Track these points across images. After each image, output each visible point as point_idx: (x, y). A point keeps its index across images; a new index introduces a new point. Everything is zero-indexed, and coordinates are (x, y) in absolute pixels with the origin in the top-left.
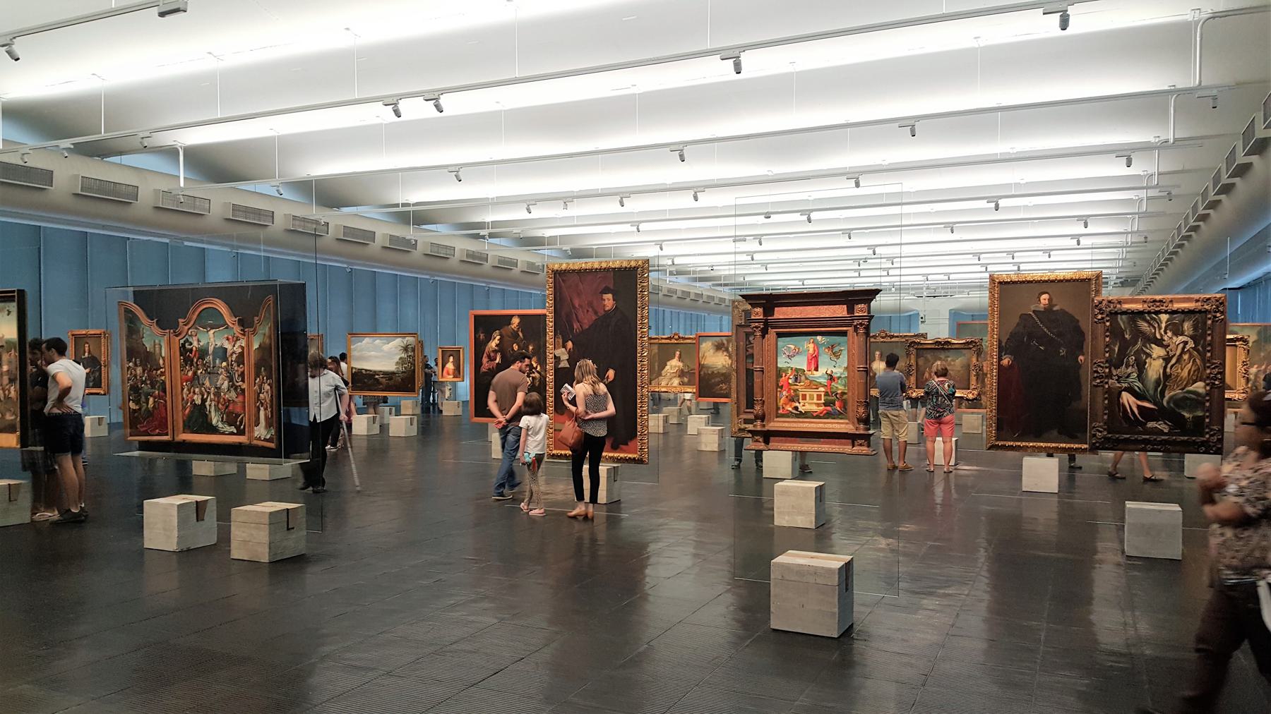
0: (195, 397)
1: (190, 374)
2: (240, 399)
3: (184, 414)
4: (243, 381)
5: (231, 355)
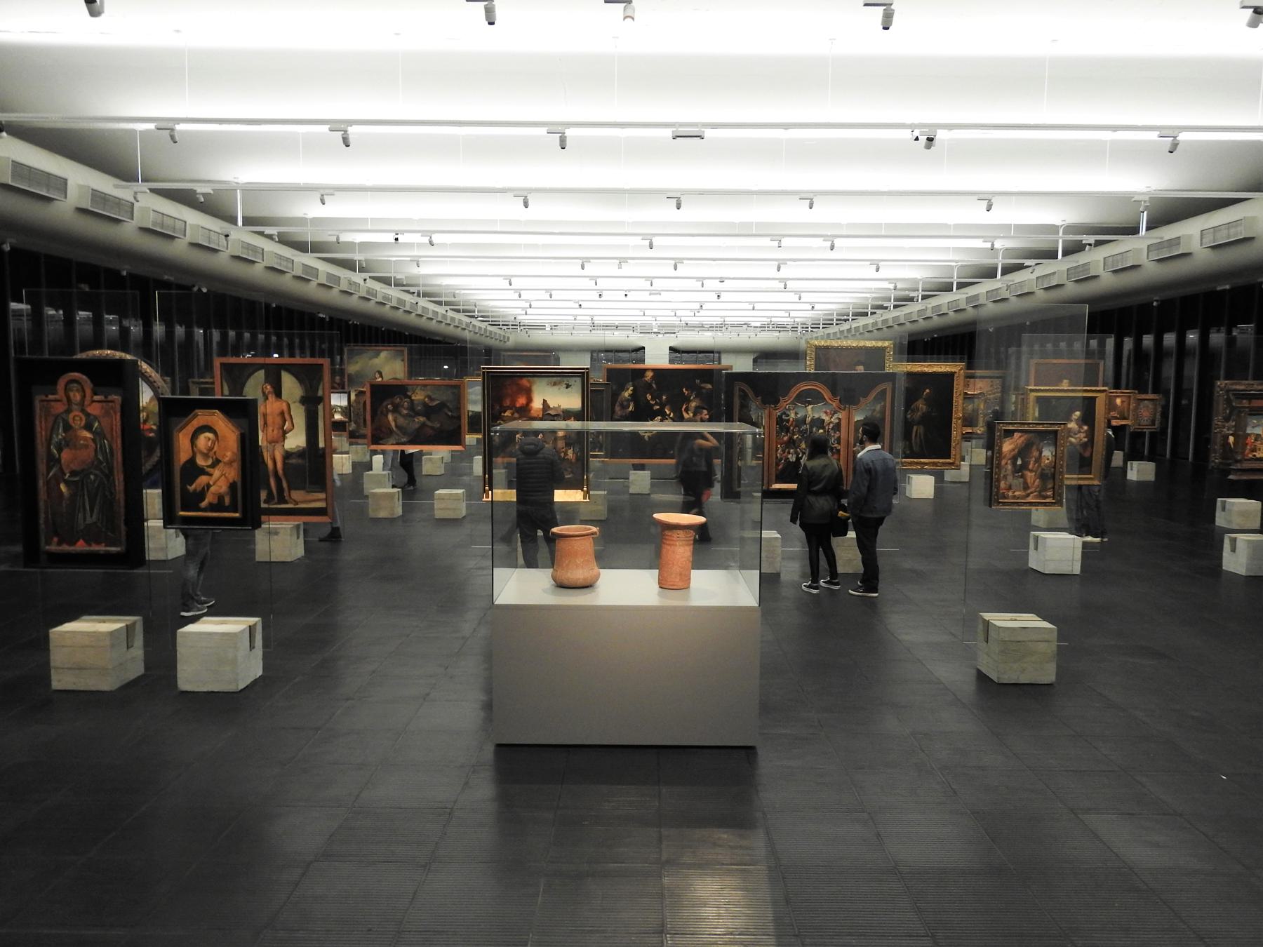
0: (790, 456)
1: (786, 438)
2: (836, 456)
3: (777, 470)
4: (839, 443)
5: (829, 424)
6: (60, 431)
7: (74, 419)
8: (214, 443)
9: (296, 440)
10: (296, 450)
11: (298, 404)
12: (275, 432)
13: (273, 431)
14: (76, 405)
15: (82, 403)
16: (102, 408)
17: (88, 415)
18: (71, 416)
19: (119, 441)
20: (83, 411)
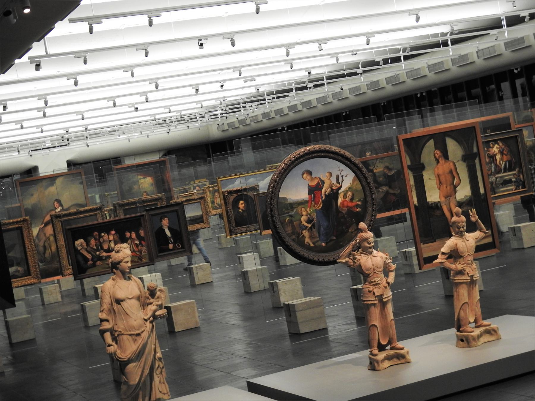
10: (465, 199)
11: (461, 162)
12: (448, 188)
13: (447, 187)
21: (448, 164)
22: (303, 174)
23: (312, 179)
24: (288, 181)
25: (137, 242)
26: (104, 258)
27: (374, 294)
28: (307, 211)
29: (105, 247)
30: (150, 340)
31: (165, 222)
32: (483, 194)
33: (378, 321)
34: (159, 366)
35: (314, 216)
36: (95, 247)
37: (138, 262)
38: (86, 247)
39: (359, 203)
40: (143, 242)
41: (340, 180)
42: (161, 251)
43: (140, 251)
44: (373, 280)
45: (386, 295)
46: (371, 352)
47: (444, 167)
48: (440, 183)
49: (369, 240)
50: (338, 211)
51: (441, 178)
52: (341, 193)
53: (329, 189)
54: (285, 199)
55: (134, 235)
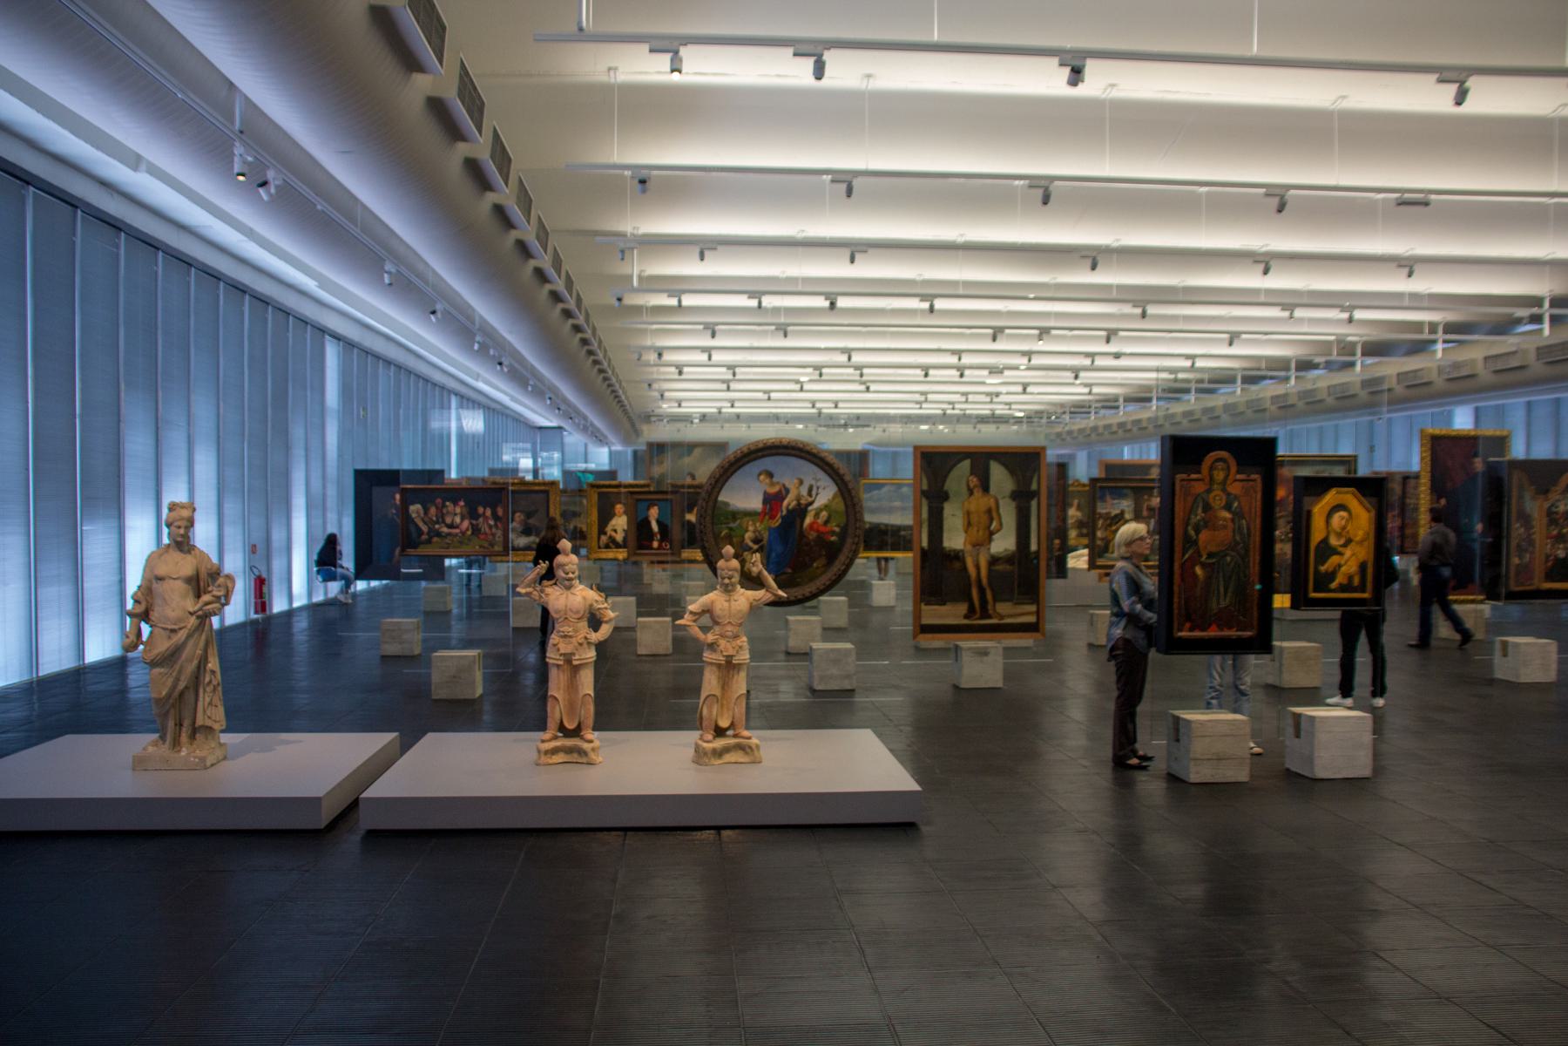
6: (1200, 510)
7: (1215, 499)
8: (1347, 521)
9: (1004, 543)
11: (1008, 501)
12: (981, 533)
13: (978, 531)
14: (1219, 484)
15: (1224, 483)
16: (1243, 487)
17: (1229, 494)
18: (1212, 495)
19: (1258, 521)
20: (1224, 490)
21: (986, 499)
22: (760, 474)
23: (772, 484)
24: (735, 480)
25: (492, 523)
26: (443, 534)
27: (558, 650)
28: (756, 527)
29: (448, 520)
30: (191, 643)
31: (654, 513)
32: (1035, 553)
33: (562, 692)
34: (210, 682)
35: (766, 535)
36: (434, 519)
37: (488, 548)
38: (422, 515)
39: (837, 529)
40: (499, 524)
41: (814, 493)
42: (641, 547)
43: (493, 535)
44: (561, 629)
45: (580, 655)
46: (701, 735)
47: (979, 502)
48: (969, 524)
49: (567, 567)
50: (802, 535)
51: (971, 517)
52: (811, 511)
53: (795, 503)
54: (727, 504)
55: (489, 512)
